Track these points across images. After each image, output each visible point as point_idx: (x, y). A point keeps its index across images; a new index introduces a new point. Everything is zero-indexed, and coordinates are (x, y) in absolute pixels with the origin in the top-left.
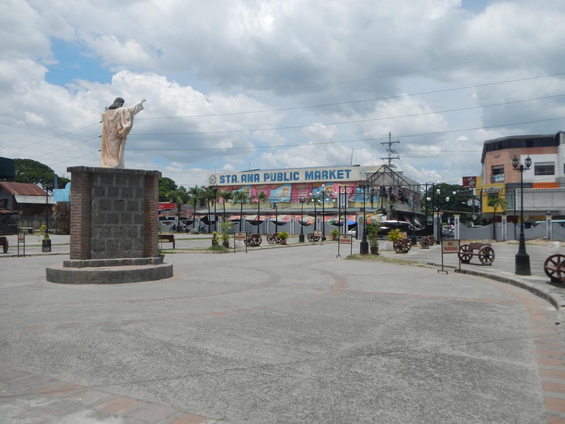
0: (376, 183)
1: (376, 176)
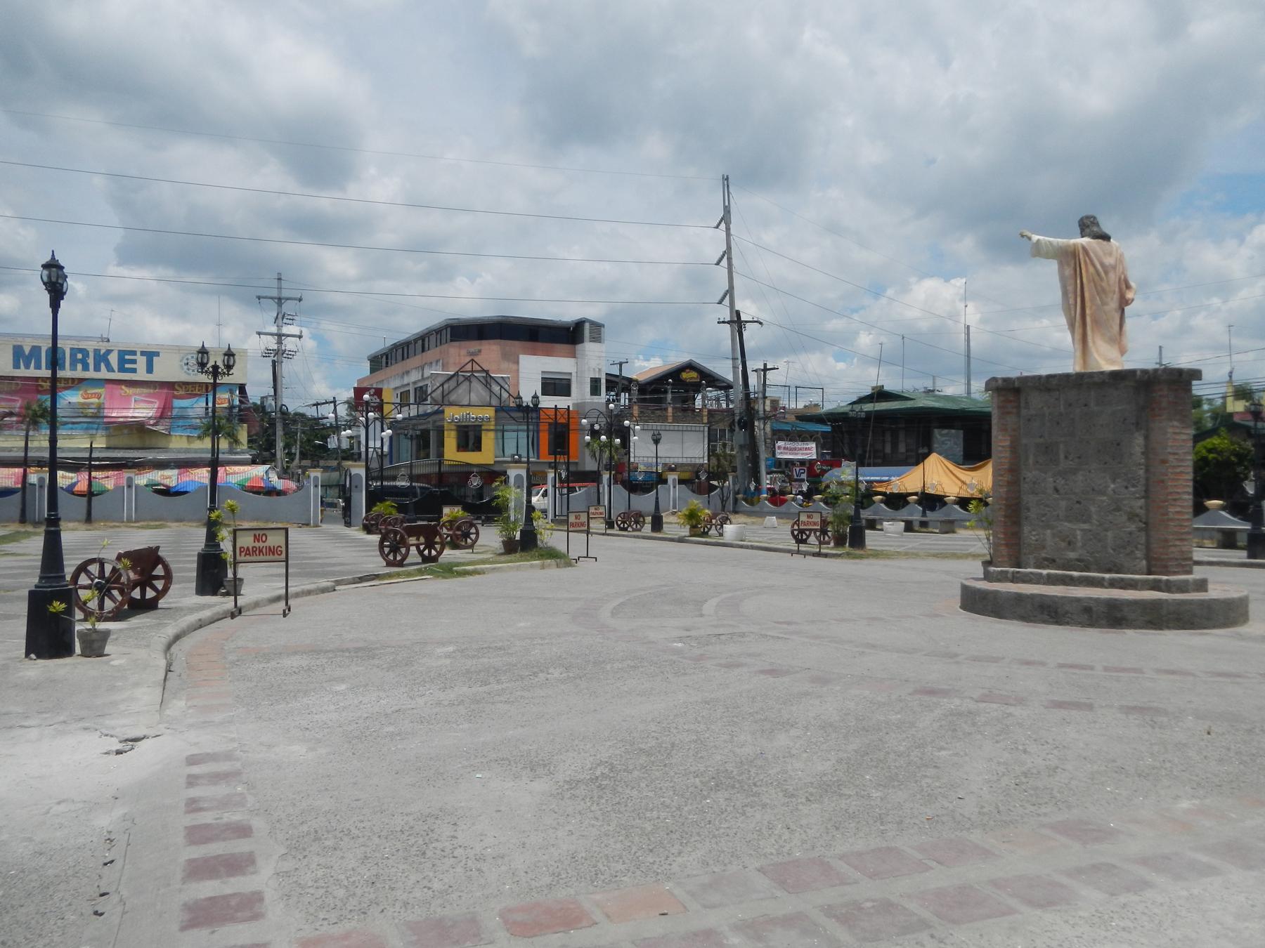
0: (453, 397)
1: (453, 383)
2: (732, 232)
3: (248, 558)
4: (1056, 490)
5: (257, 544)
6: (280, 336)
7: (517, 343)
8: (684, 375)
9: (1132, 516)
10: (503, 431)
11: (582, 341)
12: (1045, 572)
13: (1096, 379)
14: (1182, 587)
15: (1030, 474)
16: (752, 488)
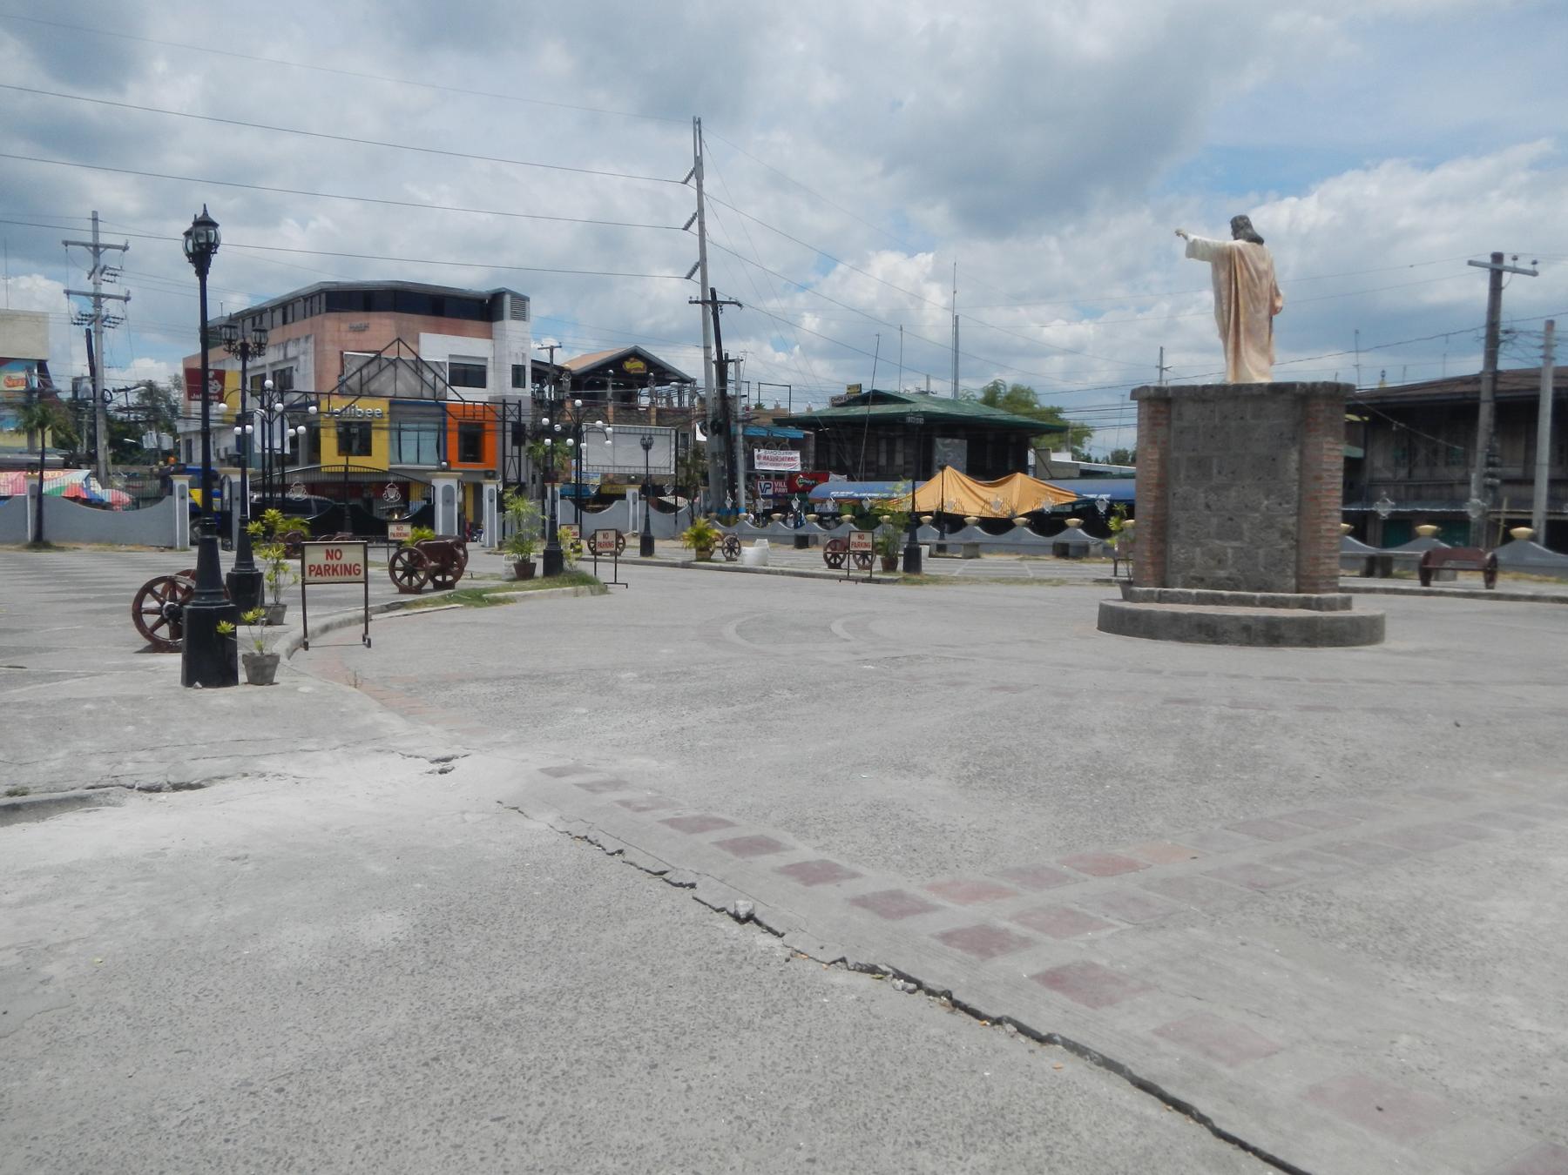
0: (374, 386)
1: (373, 368)
2: (705, 189)
3: (319, 578)
4: (1208, 506)
5: (330, 562)
6: (98, 297)
7: (416, 317)
8: (628, 365)
9: (1285, 534)
10: (400, 430)
11: (500, 318)
12: (1194, 591)
13: (1255, 391)
14: (1331, 605)
15: (1182, 489)
16: (729, 506)
